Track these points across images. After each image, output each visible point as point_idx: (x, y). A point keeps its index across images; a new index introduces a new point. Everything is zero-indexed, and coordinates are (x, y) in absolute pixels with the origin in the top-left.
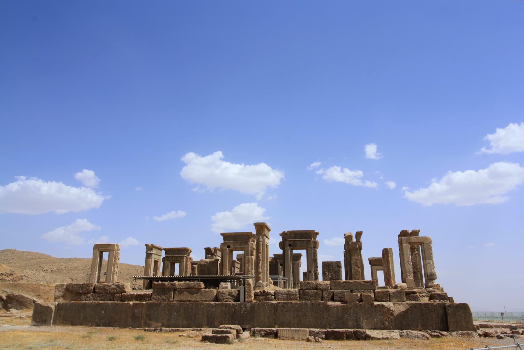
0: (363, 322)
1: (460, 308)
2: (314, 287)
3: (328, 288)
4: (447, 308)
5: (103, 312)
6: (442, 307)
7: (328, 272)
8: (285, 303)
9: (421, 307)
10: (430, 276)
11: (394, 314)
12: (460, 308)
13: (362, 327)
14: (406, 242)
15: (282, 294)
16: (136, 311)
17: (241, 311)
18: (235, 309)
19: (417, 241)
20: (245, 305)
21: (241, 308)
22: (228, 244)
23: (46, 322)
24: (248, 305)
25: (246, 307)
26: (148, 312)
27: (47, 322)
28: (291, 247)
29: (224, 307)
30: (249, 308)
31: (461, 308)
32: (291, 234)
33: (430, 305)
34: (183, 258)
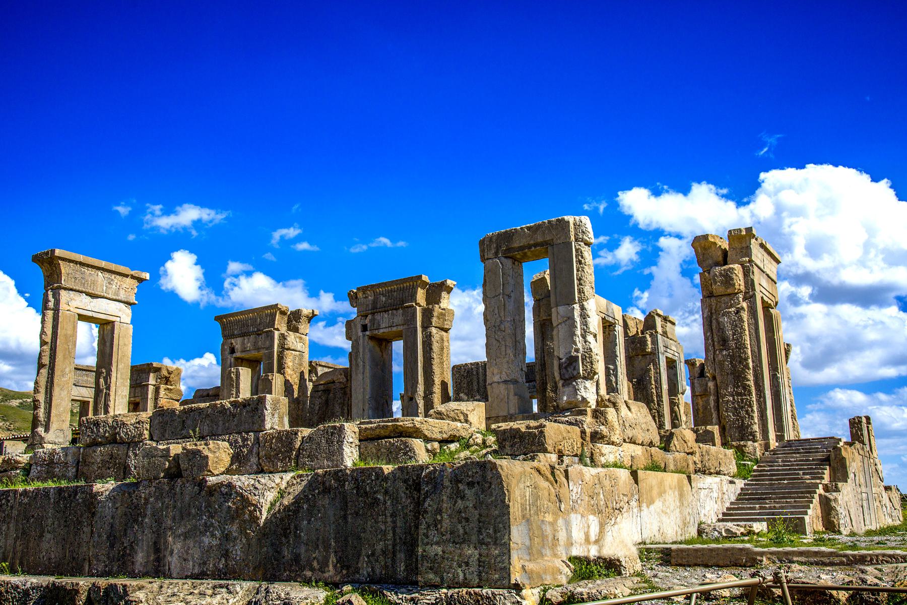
0: (172, 553)
1: (468, 484)
2: (107, 435)
3: (141, 435)
6: (410, 483)
9: (344, 485)
10: (566, 368)
11: (258, 519)
12: (468, 484)
13: (169, 569)
14: (496, 254)
19: (532, 242)
22: (232, 344)
28: (368, 333)
31: (471, 485)
32: (366, 297)
33: (373, 478)
34: (146, 388)
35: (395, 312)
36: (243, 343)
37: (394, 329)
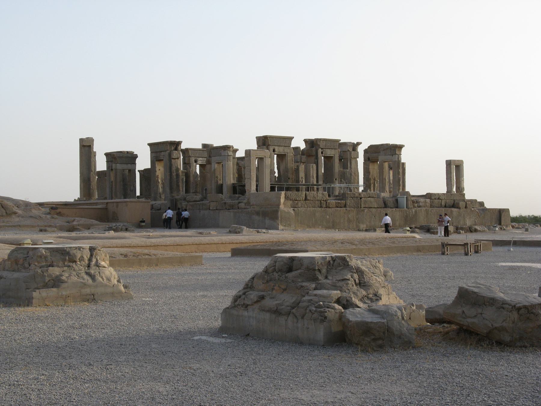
4: (501, 212)
5: (328, 217)
7: (344, 180)
8: (432, 209)
15: (422, 202)
16: (350, 215)
17: (410, 215)
18: (407, 214)
20: (412, 211)
21: (410, 213)
23: (290, 225)
24: (414, 210)
25: (412, 212)
26: (357, 217)
27: (291, 226)
29: (401, 212)
30: (414, 213)
35: (332, 150)
36: (279, 149)
37: (331, 155)
